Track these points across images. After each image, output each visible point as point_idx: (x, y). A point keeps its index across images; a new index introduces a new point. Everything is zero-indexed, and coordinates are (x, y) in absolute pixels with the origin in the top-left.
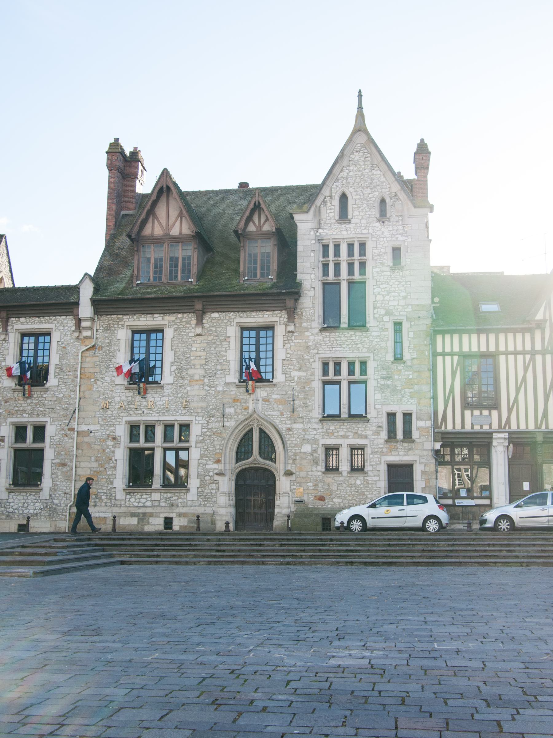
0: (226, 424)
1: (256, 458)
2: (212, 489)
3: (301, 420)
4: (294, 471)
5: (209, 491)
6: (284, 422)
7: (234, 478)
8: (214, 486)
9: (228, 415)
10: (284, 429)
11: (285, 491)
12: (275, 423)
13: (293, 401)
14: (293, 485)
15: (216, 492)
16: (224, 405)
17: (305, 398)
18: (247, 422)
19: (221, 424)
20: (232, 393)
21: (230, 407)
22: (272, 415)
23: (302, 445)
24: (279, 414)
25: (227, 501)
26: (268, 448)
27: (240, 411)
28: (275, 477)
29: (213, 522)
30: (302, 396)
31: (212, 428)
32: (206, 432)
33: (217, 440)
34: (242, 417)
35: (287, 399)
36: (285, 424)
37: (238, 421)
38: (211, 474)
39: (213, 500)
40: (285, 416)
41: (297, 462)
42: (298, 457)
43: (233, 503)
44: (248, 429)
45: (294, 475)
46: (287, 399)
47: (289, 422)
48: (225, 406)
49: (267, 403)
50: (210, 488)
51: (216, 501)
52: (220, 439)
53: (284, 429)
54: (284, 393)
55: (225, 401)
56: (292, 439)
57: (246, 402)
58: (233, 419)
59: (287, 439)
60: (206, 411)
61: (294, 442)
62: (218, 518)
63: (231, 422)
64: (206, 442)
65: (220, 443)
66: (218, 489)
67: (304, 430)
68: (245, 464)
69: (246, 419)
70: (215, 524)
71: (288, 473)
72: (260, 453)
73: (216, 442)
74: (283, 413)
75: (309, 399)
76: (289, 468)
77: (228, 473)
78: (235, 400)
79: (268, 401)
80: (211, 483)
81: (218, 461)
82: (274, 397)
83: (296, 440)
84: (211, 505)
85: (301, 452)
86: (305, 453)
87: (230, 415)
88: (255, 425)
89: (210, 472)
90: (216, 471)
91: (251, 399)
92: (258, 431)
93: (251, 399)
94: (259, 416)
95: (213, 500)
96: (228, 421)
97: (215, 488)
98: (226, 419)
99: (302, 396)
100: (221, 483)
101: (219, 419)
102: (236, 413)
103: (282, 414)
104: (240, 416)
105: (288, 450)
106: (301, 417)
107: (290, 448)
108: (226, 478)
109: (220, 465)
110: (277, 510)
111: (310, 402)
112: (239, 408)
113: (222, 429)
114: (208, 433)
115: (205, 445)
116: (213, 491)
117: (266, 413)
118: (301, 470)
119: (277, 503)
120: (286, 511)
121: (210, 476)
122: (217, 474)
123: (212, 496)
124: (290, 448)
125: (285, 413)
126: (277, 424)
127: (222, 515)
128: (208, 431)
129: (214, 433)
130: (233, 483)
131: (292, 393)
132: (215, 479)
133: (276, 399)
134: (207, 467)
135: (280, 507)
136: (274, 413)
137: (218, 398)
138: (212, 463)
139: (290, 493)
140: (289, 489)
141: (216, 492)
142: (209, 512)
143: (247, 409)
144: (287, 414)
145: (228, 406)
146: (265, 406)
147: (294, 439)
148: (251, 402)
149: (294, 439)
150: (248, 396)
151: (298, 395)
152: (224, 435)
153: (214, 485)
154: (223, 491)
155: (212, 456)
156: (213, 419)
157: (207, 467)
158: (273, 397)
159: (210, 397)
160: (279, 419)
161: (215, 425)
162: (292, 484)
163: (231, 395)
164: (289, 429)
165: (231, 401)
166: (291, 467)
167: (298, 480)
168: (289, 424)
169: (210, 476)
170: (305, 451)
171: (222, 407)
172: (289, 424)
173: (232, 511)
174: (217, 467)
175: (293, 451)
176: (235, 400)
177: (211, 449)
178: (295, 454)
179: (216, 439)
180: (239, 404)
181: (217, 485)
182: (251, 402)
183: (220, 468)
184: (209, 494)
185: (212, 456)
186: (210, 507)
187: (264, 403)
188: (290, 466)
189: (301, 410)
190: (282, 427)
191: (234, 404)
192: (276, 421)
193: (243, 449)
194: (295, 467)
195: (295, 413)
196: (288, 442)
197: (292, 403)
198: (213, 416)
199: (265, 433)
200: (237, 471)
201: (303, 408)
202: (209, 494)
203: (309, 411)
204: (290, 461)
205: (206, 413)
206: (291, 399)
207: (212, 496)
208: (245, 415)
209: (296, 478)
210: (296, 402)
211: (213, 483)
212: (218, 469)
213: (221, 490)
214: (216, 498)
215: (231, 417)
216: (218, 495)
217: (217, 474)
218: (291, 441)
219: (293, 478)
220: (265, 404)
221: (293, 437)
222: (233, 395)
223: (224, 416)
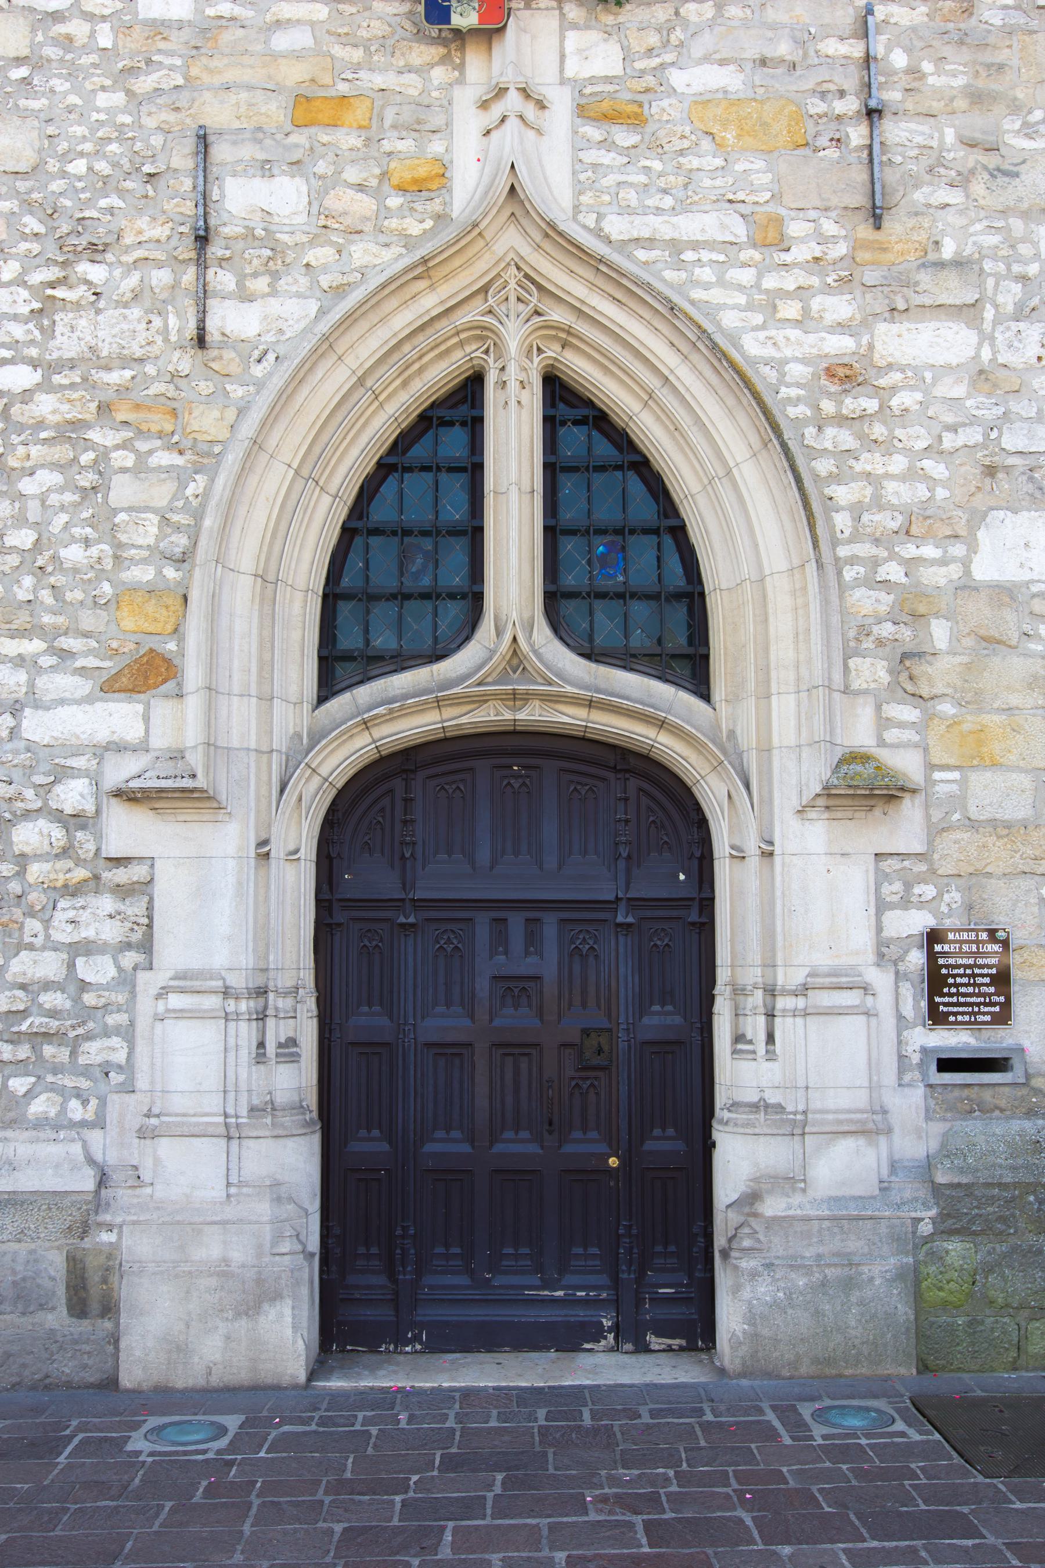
0: (229, 319)
1: (513, 659)
2: (86, 948)
3: (954, 290)
4: (907, 764)
5: (49, 966)
6: (790, 310)
7: (299, 833)
8: (99, 919)
9: (250, 234)
10: (797, 371)
11: (823, 960)
12: (712, 310)
13: (872, 114)
14: (905, 903)
15: (126, 981)
16: (204, 141)
17: (978, 98)
18: (429, 303)
19: (180, 323)
20: (281, 41)
21: (265, 168)
22: (676, 247)
23: (978, 519)
24: (740, 230)
25: (244, 1070)
26: (633, 562)
27: (364, 205)
28: (701, 823)
29: (91, 1293)
30: (947, 78)
31: (94, 359)
32: (27, 396)
33: (140, 469)
34: (376, 258)
35: (817, 107)
36: (805, 321)
37: (340, 291)
38: (73, 795)
39: (93, 1052)
40: (800, 253)
41: (940, 673)
42: (940, 633)
43: (297, 1080)
44: (437, 376)
45: (911, 810)
46: (817, 107)
47: (839, 307)
48: (220, 152)
49: (624, 137)
50: (63, 934)
51: (128, 1068)
52: (164, 458)
53: (797, 371)
54: (784, 49)
55: (216, 113)
56: (870, 462)
57: (416, 128)
58: (295, 281)
59: (824, 466)
60: (28, 205)
61: (897, 492)
62: (139, 1246)
63: (274, 306)
64: (27, 486)
65: (161, 494)
66: (146, 946)
67: (982, 377)
68: (407, 707)
69: (424, 269)
70: (109, 1308)
71: (862, 790)
72: (556, 601)
73: (123, 491)
74: (778, 222)
75: (1015, 108)
76: (860, 734)
77: (245, 785)
78: (311, 108)
79: (636, 120)
80: (72, 891)
81: (147, 673)
82: (693, 79)
83: (911, 475)
84: (76, 1110)
85: (967, 586)
86: (1005, 594)
87: (269, 240)
88: (514, 335)
89: (61, 774)
90: (121, 771)
91: (465, 98)
92: (533, 399)
93: (465, 98)
94: (552, 232)
95: (93, 1052)
96: (246, 297)
97: (111, 932)
98: (222, 279)
99: (947, 78)
100: (172, 890)
101: (161, 277)
102: (324, 226)
103: (770, 236)
104: (361, 252)
105: (839, 564)
106: (959, 264)
107: (864, 549)
108: (228, 840)
109: (162, 709)
110: (737, 1160)
111: (1029, 131)
112: (352, 174)
113: (184, 362)
114: (46, 405)
115: (20, 520)
116: (97, 970)
117: (617, 227)
118: (977, 757)
119: (736, 1077)
120: (843, 1168)
121: (58, 816)
122: (127, 796)
123: (86, 1018)
124: (864, 549)
125: (796, 228)
126: (730, 319)
127: (183, 1224)
128: (46, 386)
129: (104, 409)
130: (296, 884)
131: (856, 49)
132: (114, 848)
133: (703, 101)
134: (37, 727)
135: (796, 1126)
136: (689, 226)
137: (144, 84)
138: (84, 686)
139: (881, 980)
140: (860, 940)
141: (126, 981)
142: (50, 1182)
143: (429, 184)
144: (820, 233)
145: (248, 151)
146: (607, 158)
147: (898, 463)
148: (468, 122)
149: (898, 463)
150: (440, 74)
151: (914, 72)
152: (207, 422)
153: (107, 903)
154: (194, 962)
155: (88, 620)
156: (96, 273)
157: (37, 727)
158: (677, 78)
159: (73, 73)
160: (746, 276)
161: (119, 324)
162: (893, 890)
163: (275, 56)
164: (844, 376)
165: (274, 111)
166: (883, 723)
167: (955, 851)
168: (842, 327)
169: (58, 816)
170: (1011, 573)
171: (182, 158)
172: (842, 327)
173: (295, 1162)
174: (134, 732)
175: (893, 572)
176: (311, 108)
177: (74, 554)
178: (913, 608)
179: (124, 459)
180: (348, 140)
181: (136, 908)
182: (468, 122)
183: (159, 741)
184: (51, 999)
185: (88, 620)
186: (59, 1124)
187: (593, 132)
188: (865, 714)
189: (955, 197)
190: (786, 352)
191: (299, 138)
192: (716, 296)
193: (393, 564)
194: (922, 727)
195: (895, 226)
196: (843, 494)
197: (857, 134)
198: (96, 251)
199: (598, 419)
200: (341, 759)
201: (962, 181)
202: (51, 999)
203: (1025, 215)
204: (872, 671)
205: (32, 224)
206: (851, 105)
207: (86, 1018)
208: (409, 242)
209: (935, 831)
210: (893, 130)
211: (95, 884)
212: (142, 747)
213: (174, 952)
214: (128, 1033)
215: (273, 252)
216: (145, 1005)
217: (127, 796)
218: (882, 479)
219: (905, 829)
220: (606, 144)
221: (887, 447)
222: (297, 56)
223: (202, 240)
